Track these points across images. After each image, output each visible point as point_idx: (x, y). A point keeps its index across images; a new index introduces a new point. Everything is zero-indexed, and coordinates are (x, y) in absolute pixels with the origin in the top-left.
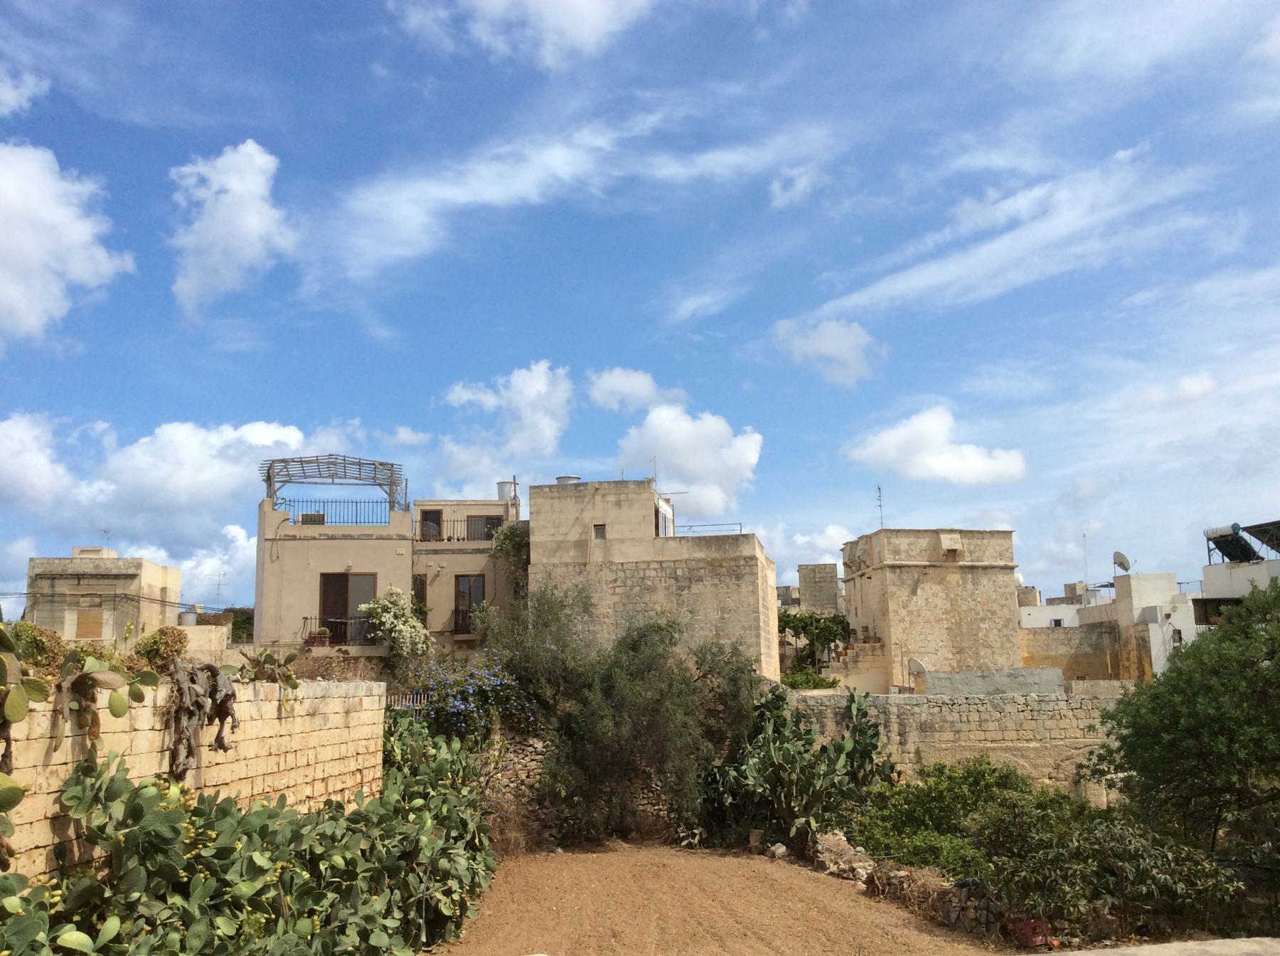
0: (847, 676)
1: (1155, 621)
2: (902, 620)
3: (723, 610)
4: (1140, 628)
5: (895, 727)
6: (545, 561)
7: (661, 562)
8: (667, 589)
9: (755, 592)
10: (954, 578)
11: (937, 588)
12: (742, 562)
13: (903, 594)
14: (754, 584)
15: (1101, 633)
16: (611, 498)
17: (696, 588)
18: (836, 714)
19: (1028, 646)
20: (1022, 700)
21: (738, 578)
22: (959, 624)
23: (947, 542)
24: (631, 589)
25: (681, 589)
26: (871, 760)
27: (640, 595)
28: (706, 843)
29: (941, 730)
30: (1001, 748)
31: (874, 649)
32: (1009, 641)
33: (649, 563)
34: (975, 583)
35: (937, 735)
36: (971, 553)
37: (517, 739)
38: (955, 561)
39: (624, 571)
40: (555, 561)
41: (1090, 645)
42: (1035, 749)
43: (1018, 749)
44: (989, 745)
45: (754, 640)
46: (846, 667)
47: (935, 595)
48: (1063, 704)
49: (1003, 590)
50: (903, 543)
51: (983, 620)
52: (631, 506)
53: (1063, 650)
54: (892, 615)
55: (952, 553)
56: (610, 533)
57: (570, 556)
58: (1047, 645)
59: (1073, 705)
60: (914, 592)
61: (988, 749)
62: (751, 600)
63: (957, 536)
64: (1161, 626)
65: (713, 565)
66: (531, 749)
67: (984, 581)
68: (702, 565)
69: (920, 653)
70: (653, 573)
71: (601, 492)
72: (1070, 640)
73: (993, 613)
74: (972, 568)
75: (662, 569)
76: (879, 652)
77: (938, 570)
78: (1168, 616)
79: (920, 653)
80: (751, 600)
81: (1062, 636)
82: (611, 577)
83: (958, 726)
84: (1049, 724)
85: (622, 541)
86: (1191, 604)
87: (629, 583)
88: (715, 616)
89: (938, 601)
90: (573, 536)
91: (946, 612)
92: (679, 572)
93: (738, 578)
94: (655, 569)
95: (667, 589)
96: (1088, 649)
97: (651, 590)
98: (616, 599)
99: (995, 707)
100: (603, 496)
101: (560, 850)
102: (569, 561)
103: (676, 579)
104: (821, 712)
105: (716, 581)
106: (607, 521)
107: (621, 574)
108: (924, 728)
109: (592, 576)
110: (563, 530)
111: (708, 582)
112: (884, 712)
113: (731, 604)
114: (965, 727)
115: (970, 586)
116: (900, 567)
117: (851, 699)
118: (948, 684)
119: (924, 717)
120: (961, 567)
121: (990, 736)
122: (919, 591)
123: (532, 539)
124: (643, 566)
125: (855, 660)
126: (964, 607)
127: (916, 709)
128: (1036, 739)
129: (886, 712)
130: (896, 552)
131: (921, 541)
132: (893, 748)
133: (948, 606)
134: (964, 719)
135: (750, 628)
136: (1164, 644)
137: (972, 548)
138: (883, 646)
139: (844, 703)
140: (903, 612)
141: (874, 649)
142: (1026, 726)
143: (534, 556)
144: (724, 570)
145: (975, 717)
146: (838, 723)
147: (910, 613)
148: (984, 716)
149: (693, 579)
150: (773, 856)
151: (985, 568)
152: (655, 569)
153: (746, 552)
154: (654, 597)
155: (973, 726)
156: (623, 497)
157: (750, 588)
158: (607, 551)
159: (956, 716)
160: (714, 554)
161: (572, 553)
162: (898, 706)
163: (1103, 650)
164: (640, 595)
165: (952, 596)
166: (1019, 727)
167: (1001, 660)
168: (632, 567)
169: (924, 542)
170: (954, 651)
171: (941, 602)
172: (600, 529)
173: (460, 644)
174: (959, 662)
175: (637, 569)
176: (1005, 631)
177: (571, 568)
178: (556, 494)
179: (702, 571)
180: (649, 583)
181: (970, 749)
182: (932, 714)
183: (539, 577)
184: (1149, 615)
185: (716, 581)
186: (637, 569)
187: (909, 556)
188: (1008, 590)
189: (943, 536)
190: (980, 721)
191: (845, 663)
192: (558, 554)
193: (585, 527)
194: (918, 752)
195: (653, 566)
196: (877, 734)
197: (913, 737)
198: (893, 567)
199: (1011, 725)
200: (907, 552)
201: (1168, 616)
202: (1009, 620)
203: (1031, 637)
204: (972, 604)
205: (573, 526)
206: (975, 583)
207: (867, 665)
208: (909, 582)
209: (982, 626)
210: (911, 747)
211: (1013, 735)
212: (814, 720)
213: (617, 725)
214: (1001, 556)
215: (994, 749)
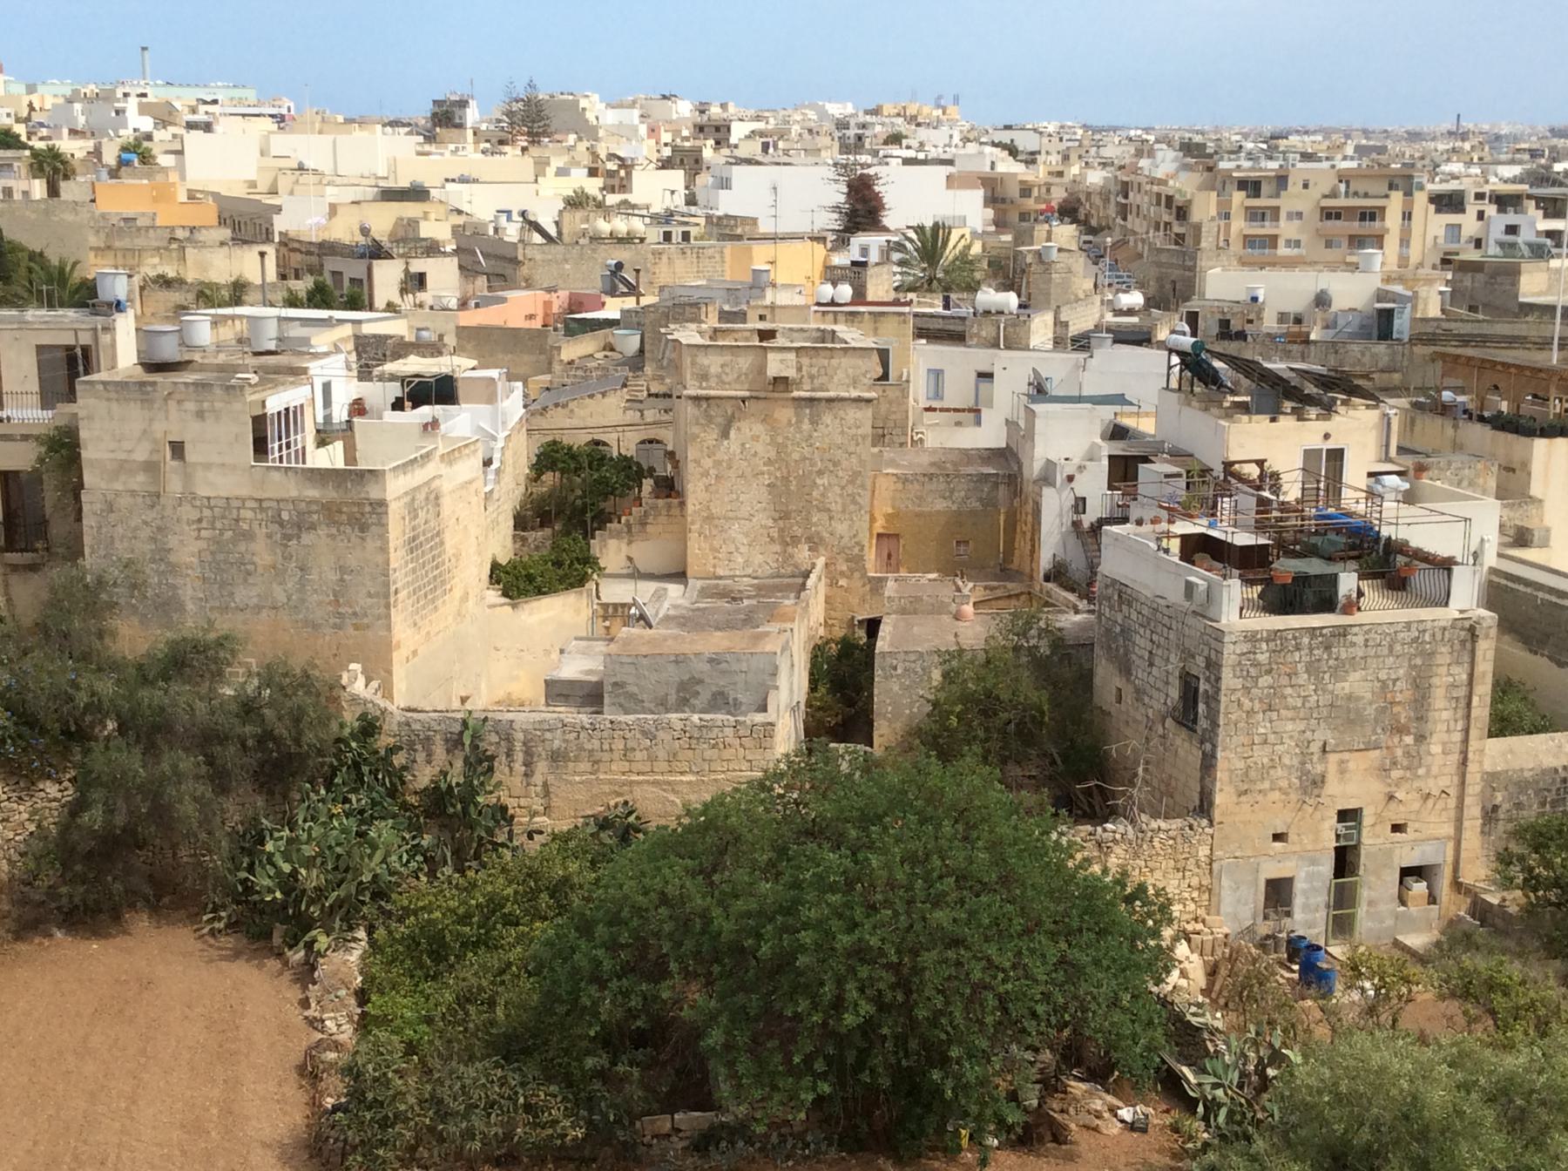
0: (630, 543)
1: (1053, 485)
2: (706, 474)
3: (342, 569)
4: (1037, 489)
5: (519, 757)
6: (103, 485)
7: (261, 501)
8: (269, 536)
9: (384, 549)
10: (785, 414)
11: (759, 428)
12: (368, 509)
13: (711, 436)
14: (383, 538)
15: (996, 485)
16: (191, 406)
17: (307, 538)
18: (447, 740)
19: (893, 499)
20: (678, 725)
21: (363, 528)
22: (786, 479)
23: (776, 365)
24: (221, 534)
25: (288, 537)
26: (476, 804)
27: (234, 541)
28: (233, 926)
29: (577, 759)
30: (648, 782)
31: (669, 507)
32: (854, 502)
33: (244, 500)
34: (814, 422)
35: (571, 765)
36: (812, 377)
37: (22, 784)
38: (787, 390)
39: (211, 508)
40: (119, 486)
41: (980, 500)
42: (689, 783)
43: (669, 783)
44: (635, 778)
45: (382, 610)
46: (630, 531)
47: (756, 438)
48: (729, 731)
49: (854, 431)
50: (713, 363)
51: (820, 473)
52: (217, 419)
53: (941, 505)
54: (691, 466)
55: (781, 382)
56: (191, 456)
57: (139, 481)
58: (920, 498)
59: (741, 733)
60: (725, 434)
61: (632, 782)
62: (380, 559)
63: (792, 356)
64: (1059, 493)
65: (331, 511)
66: (42, 794)
67: (827, 418)
68: (314, 507)
69: (727, 519)
70: (249, 514)
71: (177, 396)
72: (952, 491)
73: (836, 464)
74: (812, 400)
75: (262, 509)
76: (676, 511)
77: (762, 404)
78: (1070, 479)
79: (727, 519)
80: (380, 559)
81: (942, 486)
82: (195, 515)
83: (598, 755)
84: (709, 754)
85: (208, 466)
86: (1106, 462)
87: (218, 525)
88: (333, 577)
89: (759, 448)
90: (141, 455)
91: (769, 462)
92: (285, 515)
93: (362, 530)
94: (252, 509)
95: (269, 536)
96: (977, 505)
97: (248, 536)
98: (202, 544)
99: (645, 733)
100: (179, 402)
101: (59, 935)
102: (136, 487)
103: (281, 524)
104: (428, 738)
105: (334, 531)
106: (187, 437)
107: (207, 513)
108: (556, 757)
109: (168, 512)
110: (127, 445)
111: (322, 531)
112: (507, 739)
113: (352, 561)
114: (606, 756)
115: (806, 426)
116: (707, 398)
117: (465, 723)
118: (631, 669)
119: (556, 744)
120: (794, 399)
121: (635, 766)
122: (732, 433)
123: (86, 454)
124: (235, 504)
125: (643, 524)
126: (796, 456)
127: (548, 735)
128: (691, 771)
129: (509, 739)
130: (704, 377)
131: (741, 360)
132: (517, 781)
133: (773, 455)
134: (606, 747)
135: (377, 595)
136: (1061, 515)
137: (814, 371)
138: (682, 504)
139: (457, 728)
140: (707, 463)
141: (669, 507)
142: (680, 756)
143: (88, 478)
144: (344, 517)
145: (619, 745)
146: (448, 751)
147: (718, 463)
148: (630, 744)
149: (302, 525)
150: (286, 963)
151: (830, 400)
152: (252, 509)
153: (374, 493)
154: (253, 546)
155: (616, 755)
156: (206, 405)
157: (379, 544)
158: (187, 478)
159: (596, 743)
160: (330, 494)
161: (141, 477)
162: (525, 731)
163: (995, 506)
164: (234, 541)
165: (780, 440)
166: (673, 757)
167: (841, 528)
168: (222, 503)
169: (745, 362)
170: (777, 515)
171: (763, 449)
172: (178, 449)
173: (15, 568)
174: (781, 530)
175: (228, 507)
176: (850, 489)
177: (140, 500)
178: (113, 395)
179: (315, 517)
180: (246, 527)
181: (610, 782)
182: (566, 741)
183: (98, 507)
184: (1047, 479)
185: (334, 531)
186: (228, 507)
187: (722, 383)
188: (860, 432)
189: (771, 356)
190: (626, 749)
191: (629, 526)
192: (123, 478)
193: (155, 441)
194: (545, 785)
195: (249, 504)
196: (491, 770)
197: (541, 767)
198: (697, 399)
199: (662, 754)
200: (719, 377)
201: (1070, 479)
202: (856, 474)
203: (900, 486)
204: (807, 451)
205: (139, 440)
206: (814, 422)
207: (660, 528)
208: (720, 420)
209: (819, 481)
210: (538, 779)
211: (664, 766)
212: (419, 747)
213: (110, 811)
214: (855, 383)
215: (639, 783)
